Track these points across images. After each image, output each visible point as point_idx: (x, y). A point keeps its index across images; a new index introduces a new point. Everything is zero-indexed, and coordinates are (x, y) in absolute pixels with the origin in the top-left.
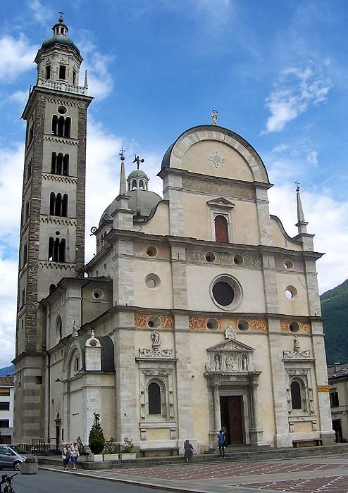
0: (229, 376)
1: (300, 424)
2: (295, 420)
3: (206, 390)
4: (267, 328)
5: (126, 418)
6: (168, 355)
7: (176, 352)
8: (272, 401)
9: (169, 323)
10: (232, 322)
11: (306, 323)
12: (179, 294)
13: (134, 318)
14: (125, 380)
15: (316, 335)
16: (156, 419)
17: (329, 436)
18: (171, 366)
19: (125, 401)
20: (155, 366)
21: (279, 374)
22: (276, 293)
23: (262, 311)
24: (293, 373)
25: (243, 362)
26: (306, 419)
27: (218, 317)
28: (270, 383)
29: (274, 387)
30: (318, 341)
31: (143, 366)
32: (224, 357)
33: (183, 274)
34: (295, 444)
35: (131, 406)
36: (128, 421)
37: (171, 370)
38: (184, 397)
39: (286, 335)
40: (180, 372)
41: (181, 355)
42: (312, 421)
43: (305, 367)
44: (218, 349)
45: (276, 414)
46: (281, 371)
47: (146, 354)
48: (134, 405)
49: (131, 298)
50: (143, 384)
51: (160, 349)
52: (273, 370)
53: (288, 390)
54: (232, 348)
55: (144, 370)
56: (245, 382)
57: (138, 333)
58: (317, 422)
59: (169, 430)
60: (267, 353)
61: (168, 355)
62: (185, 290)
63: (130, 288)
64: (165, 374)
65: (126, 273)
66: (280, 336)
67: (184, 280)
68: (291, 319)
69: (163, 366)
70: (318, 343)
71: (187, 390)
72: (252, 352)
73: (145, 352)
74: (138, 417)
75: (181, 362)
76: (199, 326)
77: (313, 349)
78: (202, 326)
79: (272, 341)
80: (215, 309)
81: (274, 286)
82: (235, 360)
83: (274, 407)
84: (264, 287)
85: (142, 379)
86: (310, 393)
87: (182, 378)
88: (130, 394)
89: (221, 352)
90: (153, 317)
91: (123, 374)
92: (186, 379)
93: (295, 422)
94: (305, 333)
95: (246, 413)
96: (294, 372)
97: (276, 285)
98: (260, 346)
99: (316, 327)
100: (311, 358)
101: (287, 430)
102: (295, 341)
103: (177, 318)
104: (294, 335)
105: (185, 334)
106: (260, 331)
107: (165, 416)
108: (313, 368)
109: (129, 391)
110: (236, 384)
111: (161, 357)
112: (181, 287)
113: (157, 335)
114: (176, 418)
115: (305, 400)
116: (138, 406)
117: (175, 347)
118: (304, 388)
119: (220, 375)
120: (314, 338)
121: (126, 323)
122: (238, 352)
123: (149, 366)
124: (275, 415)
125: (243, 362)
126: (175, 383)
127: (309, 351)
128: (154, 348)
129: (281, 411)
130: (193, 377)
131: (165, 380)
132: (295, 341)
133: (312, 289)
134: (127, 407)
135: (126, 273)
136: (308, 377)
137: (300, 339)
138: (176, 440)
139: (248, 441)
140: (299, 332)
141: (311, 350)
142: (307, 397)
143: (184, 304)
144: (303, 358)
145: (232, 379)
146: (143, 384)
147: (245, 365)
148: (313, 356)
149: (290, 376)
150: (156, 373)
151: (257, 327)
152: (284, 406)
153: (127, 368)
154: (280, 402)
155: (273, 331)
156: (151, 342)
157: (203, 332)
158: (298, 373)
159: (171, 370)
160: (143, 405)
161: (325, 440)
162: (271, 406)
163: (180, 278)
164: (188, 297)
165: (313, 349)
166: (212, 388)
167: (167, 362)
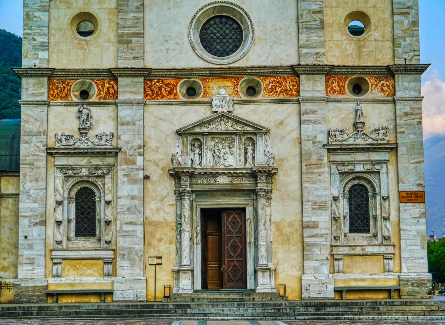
0: (214, 175)
1: (360, 259)
2: (347, 251)
3: (172, 199)
4: (298, 92)
5: (27, 242)
6: (103, 142)
7: (119, 138)
8: (299, 216)
9: (111, 91)
10: (229, 84)
11: (386, 78)
12: (130, 42)
13: (46, 86)
14: (28, 185)
15: (404, 100)
16: (82, 242)
17: (419, 283)
18: (109, 160)
19: (26, 217)
20: (84, 161)
21: (315, 171)
22: (323, 28)
23: (293, 61)
24: (347, 169)
25: (246, 153)
26: (369, 250)
27: (199, 76)
28: (298, 186)
29: (305, 194)
30: (408, 109)
31: (62, 161)
32: (209, 143)
33: (137, 8)
34: (339, 291)
35: (36, 224)
36: (31, 247)
37: (110, 167)
38: (128, 209)
39: (340, 101)
40: (124, 170)
41: (127, 143)
42: (383, 254)
43: (375, 156)
44: (197, 130)
45: (306, 240)
46: (319, 165)
47: (64, 143)
48: (43, 223)
49: (43, 55)
50: (61, 191)
51: (91, 134)
52: (303, 165)
53: (335, 199)
54: (222, 127)
55: (63, 168)
56: (247, 183)
57: (54, 110)
58: (397, 256)
59: (100, 262)
60: (295, 134)
61: (103, 142)
62: (140, 35)
63: (40, 39)
64: (99, 173)
65: (37, 14)
66: (323, 104)
67: (138, 19)
68: (352, 73)
69: (96, 161)
70: (406, 114)
71: (133, 198)
72: (265, 133)
73: (63, 139)
74: (50, 241)
75: (125, 153)
76: (164, 92)
77: (396, 125)
78: (170, 93)
79: (306, 113)
80: (198, 64)
81: (317, 16)
82: (230, 148)
83: (303, 228)
84: (298, 18)
85: (59, 182)
86: (386, 204)
87: (126, 179)
88: (35, 205)
89: (202, 134)
90: (83, 84)
91: (25, 175)
92: (134, 181)
93: (344, 255)
94: (380, 95)
95: (250, 237)
96: (351, 167)
97: (321, 12)
98: (281, 123)
99: (406, 84)
100: (391, 138)
101: (325, 270)
102: (356, 111)
103: (121, 81)
104: (355, 101)
105: (134, 107)
106: (281, 97)
107: (100, 240)
108: (393, 158)
109: (35, 201)
110: (229, 187)
111: (91, 146)
112: (133, 30)
113: (85, 111)
114: (113, 242)
115: (375, 217)
116: (51, 223)
117: (117, 129)
118: (374, 195)
119: (192, 175)
120: (399, 105)
121: (33, 94)
122: (235, 134)
123: (72, 161)
124: (303, 242)
125: (246, 153)
126: (115, 189)
127: (386, 128)
128: (83, 132)
129: (316, 236)
130: (147, 177)
131: (99, 183)
132: (356, 111)
133: (402, 14)
134: (29, 226)
135: (37, 14)
136: (383, 177)
137: (363, 106)
138: (113, 278)
139: (250, 285)
140: (368, 95)
141: (391, 127)
142: (379, 213)
143: (134, 58)
144: (370, 141)
145: (223, 180)
146: (61, 191)
147: (250, 156)
148: (396, 137)
149: (342, 173)
150: (85, 172)
151: (279, 90)
152: (321, 225)
153: (33, 164)
154: (314, 219)
155: (308, 95)
156: (77, 122)
157: (171, 104)
158: (359, 168)
159: (110, 167)
160: (59, 223)
161: (405, 289)
162: (298, 225)
163: (132, 15)
164: (148, 47)
165: (396, 125)
166: (180, 195)
167: (103, 153)
